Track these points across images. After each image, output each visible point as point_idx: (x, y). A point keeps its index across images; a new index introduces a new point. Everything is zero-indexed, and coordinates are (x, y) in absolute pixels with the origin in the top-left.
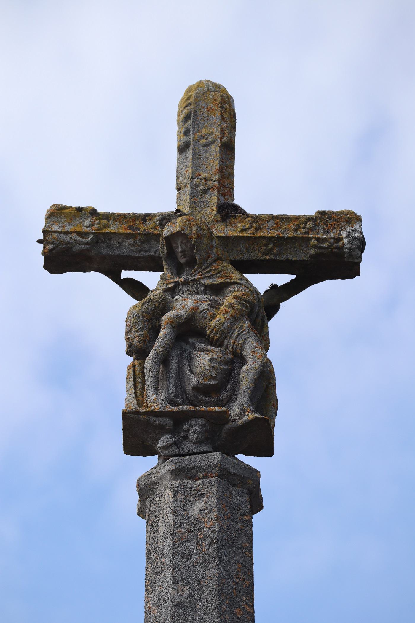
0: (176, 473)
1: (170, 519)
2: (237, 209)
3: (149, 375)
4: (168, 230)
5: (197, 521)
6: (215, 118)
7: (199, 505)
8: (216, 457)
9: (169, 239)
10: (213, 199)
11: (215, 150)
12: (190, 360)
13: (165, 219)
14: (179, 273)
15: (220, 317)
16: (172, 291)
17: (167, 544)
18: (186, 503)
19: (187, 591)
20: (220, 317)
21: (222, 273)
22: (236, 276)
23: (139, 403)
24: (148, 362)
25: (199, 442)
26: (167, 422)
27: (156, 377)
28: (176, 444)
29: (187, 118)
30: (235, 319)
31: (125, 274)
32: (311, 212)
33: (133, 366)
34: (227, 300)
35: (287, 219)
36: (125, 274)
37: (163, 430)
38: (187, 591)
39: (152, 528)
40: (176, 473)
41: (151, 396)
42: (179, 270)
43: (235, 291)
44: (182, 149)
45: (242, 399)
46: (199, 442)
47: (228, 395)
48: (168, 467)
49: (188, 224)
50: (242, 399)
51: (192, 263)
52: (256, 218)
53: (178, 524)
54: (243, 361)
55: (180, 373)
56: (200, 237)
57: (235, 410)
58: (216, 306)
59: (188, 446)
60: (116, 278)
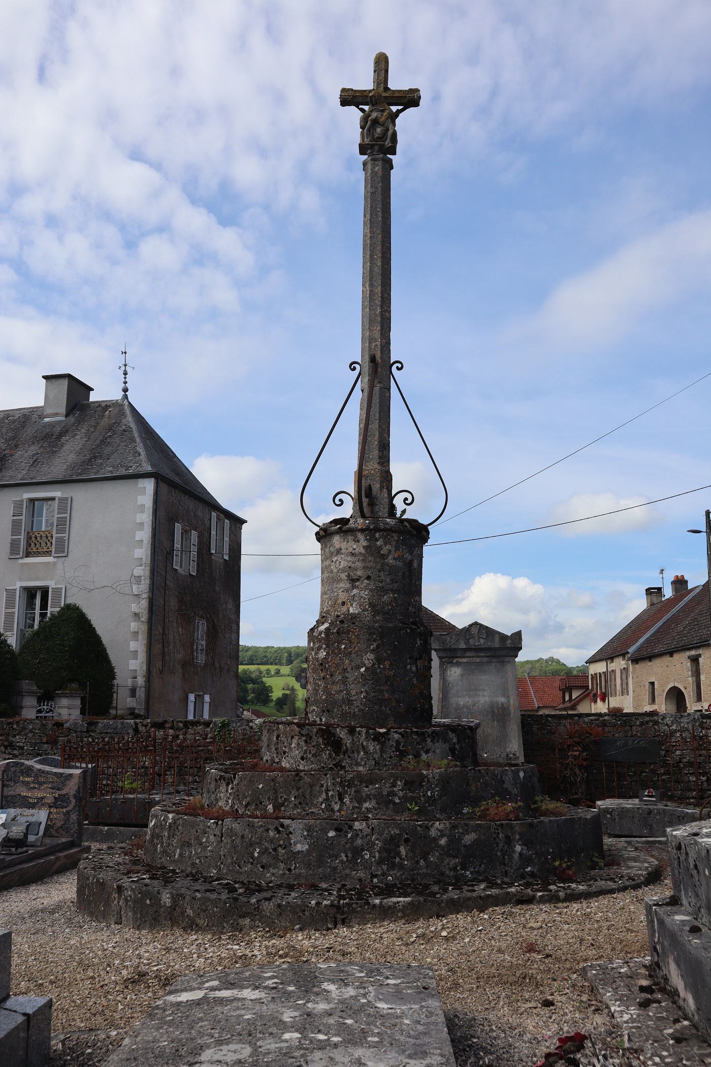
0: (371, 160)
1: (370, 171)
2: (389, 89)
3: (365, 134)
4: (370, 95)
5: (377, 172)
6: (383, 63)
7: (377, 168)
8: (381, 155)
9: (371, 97)
10: (382, 85)
11: (383, 72)
12: (376, 130)
13: (370, 91)
14: (373, 106)
15: (383, 118)
16: (371, 111)
17: (369, 178)
18: (374, 167)
19: (374, 190)
20: (383, 118)
21: (384, 106)
22: (387, 107)
23: (363, 141)
24: (365, 131)
25: (377, 152)
26: (369, 146)
27: (367, 135)
28: (372, 152)
29: (376, 63)
30: (387, 119)
31: (360, 107)
32: (407, 89)
33: (362, 132)
34: (385, 114)
35: (401, 91)
36: (360, 107)
37: (368, 149)
38: (374, 190)
39: (366, 174)
40: (371, 160)
41: (366, 140)
42: (373, 105)
43: (387, 111)
44: (375, 72)
45: (388, 140)
46: (377, 152)
47: (373, 559)
48: (370, 158)
49: (375, 93)
50: (388, 140)
51: (376, 104)
52: (393, 91)
53: (372, 173)
54: (389, 130)
55: (373, 133)
56: (378, 96)
57: (386, 143)
58: (382, 115)
59: (375, 153)
60: (358, 108)
